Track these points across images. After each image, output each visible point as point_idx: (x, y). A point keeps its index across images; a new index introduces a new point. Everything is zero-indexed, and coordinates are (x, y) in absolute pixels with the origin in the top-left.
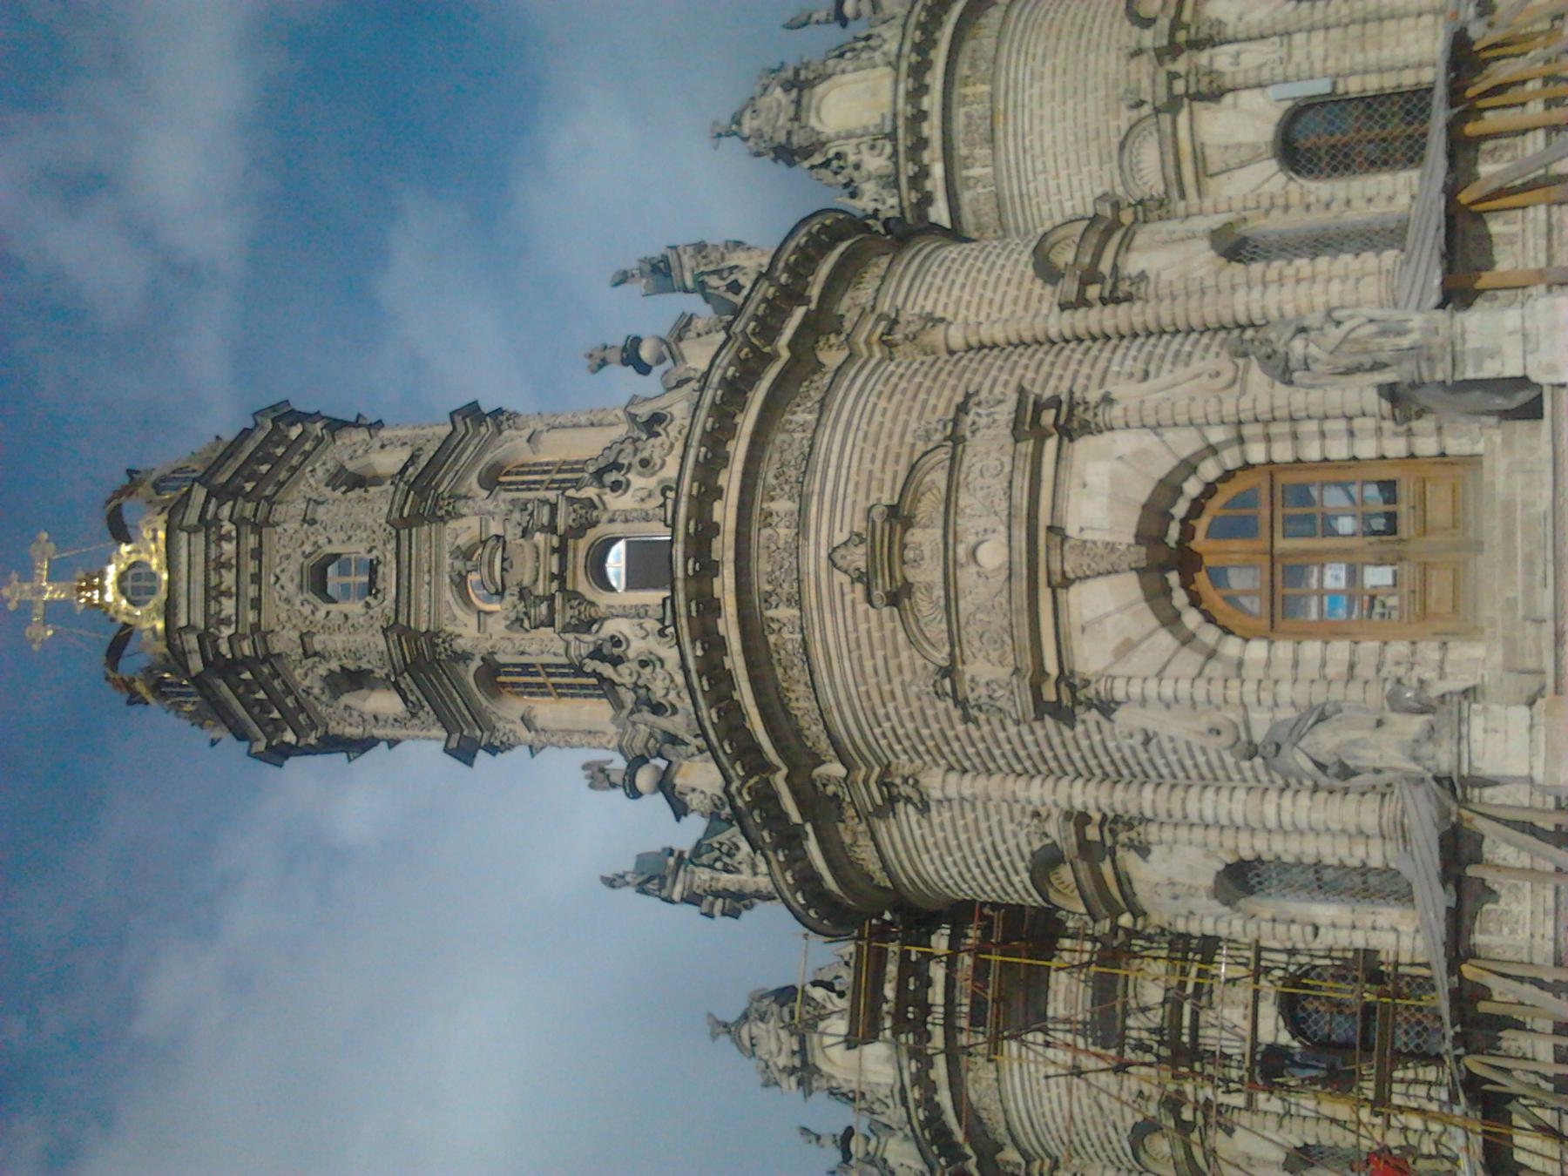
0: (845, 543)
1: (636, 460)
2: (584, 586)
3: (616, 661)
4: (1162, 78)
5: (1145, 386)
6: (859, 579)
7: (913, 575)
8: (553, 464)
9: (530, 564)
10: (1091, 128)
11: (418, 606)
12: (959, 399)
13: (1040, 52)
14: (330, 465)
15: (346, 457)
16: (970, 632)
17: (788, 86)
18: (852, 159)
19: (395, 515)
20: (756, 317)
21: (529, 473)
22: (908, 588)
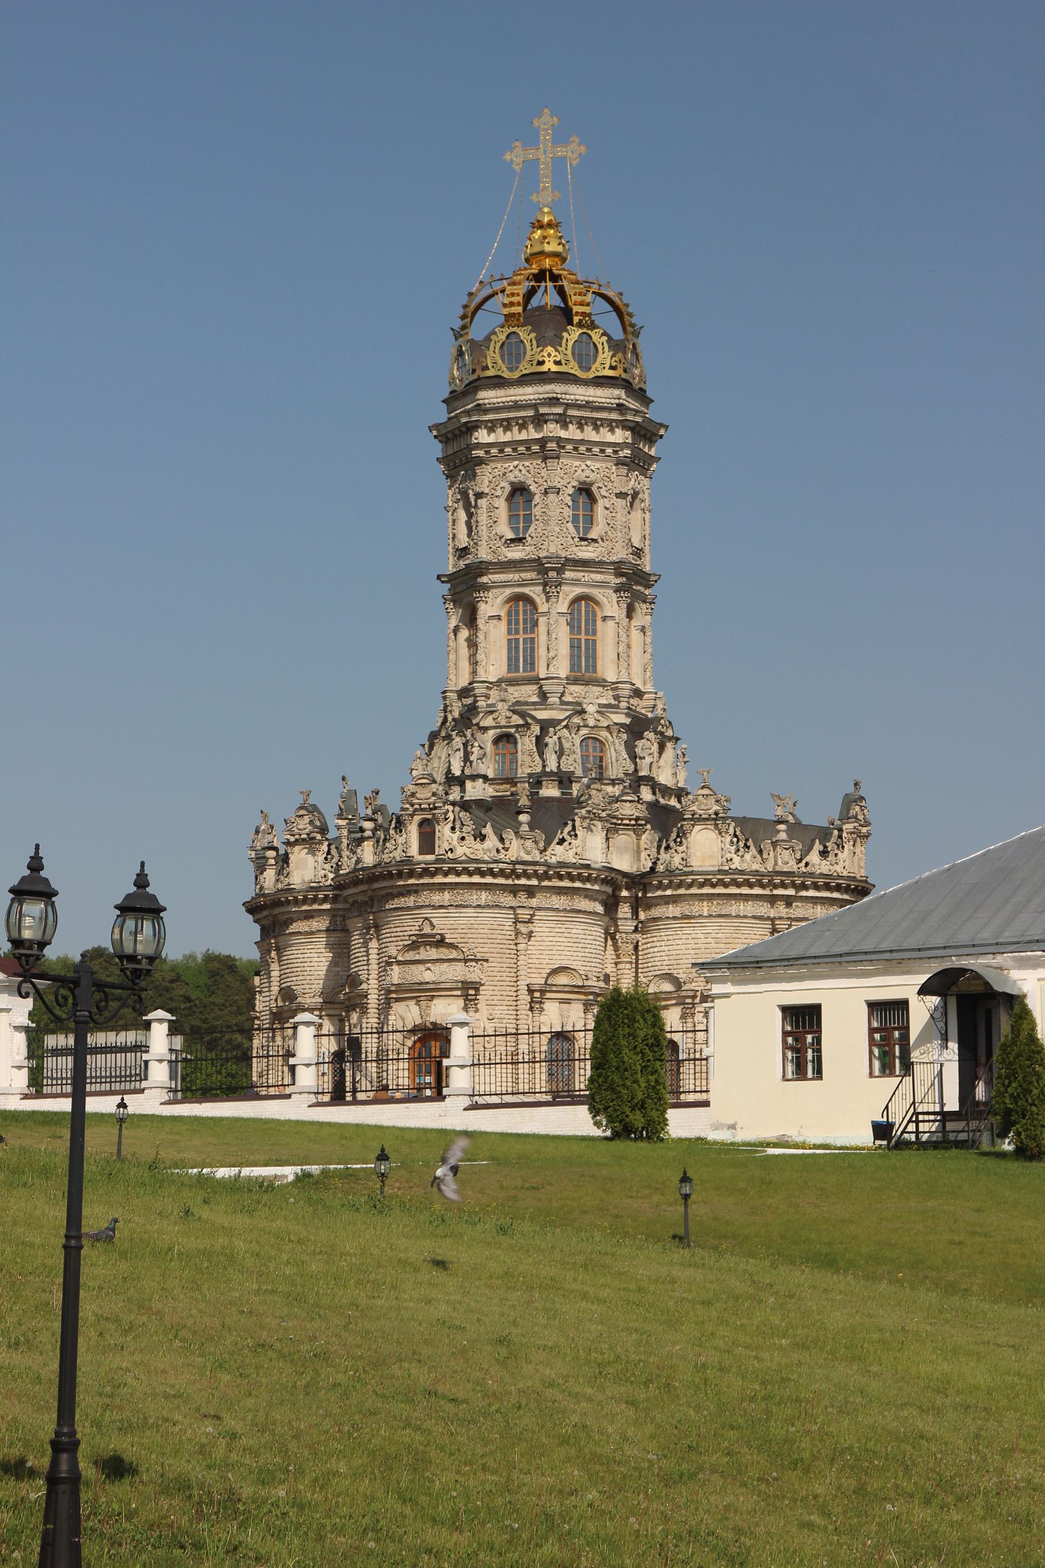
0: (431, 924)
1: (464, 834)
2: (417, 819)
3: (395, 828)
4: (691, 994)
5: (486, 1020)
6: (420, 930)
7: (422, 949)
8: (595, 633)
9: (423, 796)
10: (681, 962)
11: (502, 573)
12: (486, 956)
13: (718, 936)
14: (593, 477)
15: (600, 485)
16: (406, 968)
17: (716, 814)
18: (680, 849)
19: (544, 561)
20: (525, 871)
21: (587, 620)
22: (418, 948)
